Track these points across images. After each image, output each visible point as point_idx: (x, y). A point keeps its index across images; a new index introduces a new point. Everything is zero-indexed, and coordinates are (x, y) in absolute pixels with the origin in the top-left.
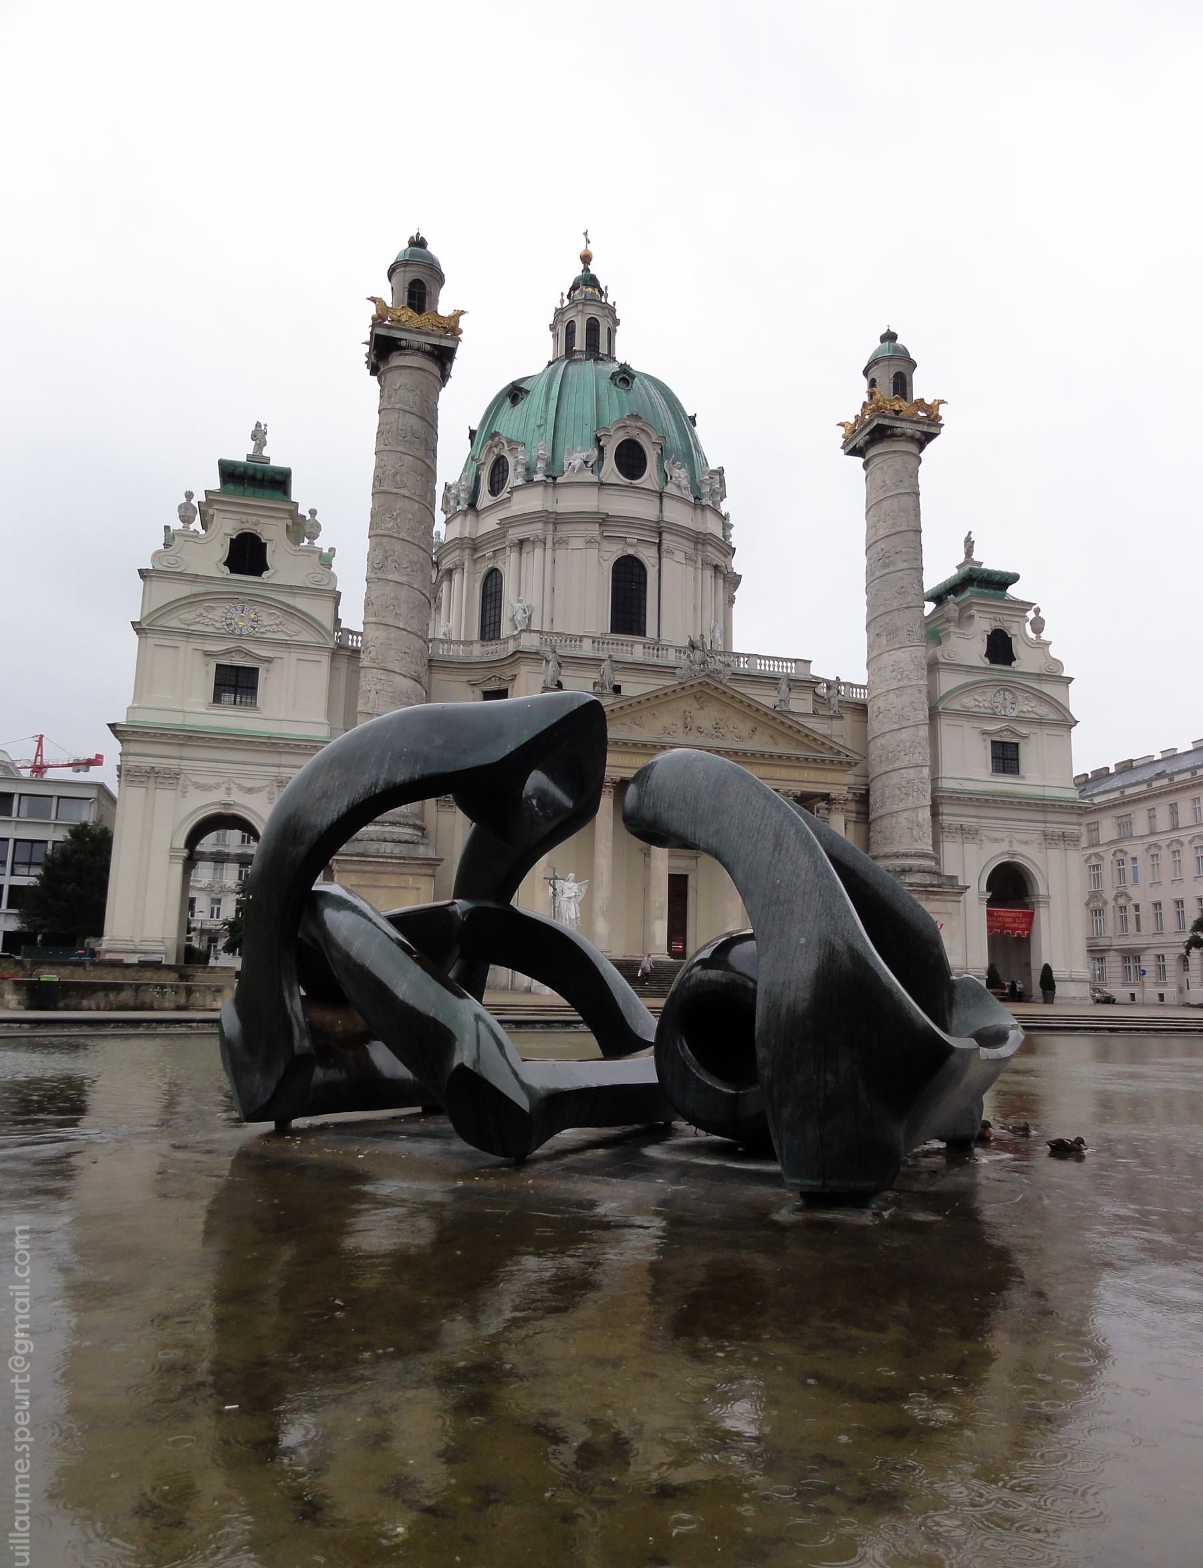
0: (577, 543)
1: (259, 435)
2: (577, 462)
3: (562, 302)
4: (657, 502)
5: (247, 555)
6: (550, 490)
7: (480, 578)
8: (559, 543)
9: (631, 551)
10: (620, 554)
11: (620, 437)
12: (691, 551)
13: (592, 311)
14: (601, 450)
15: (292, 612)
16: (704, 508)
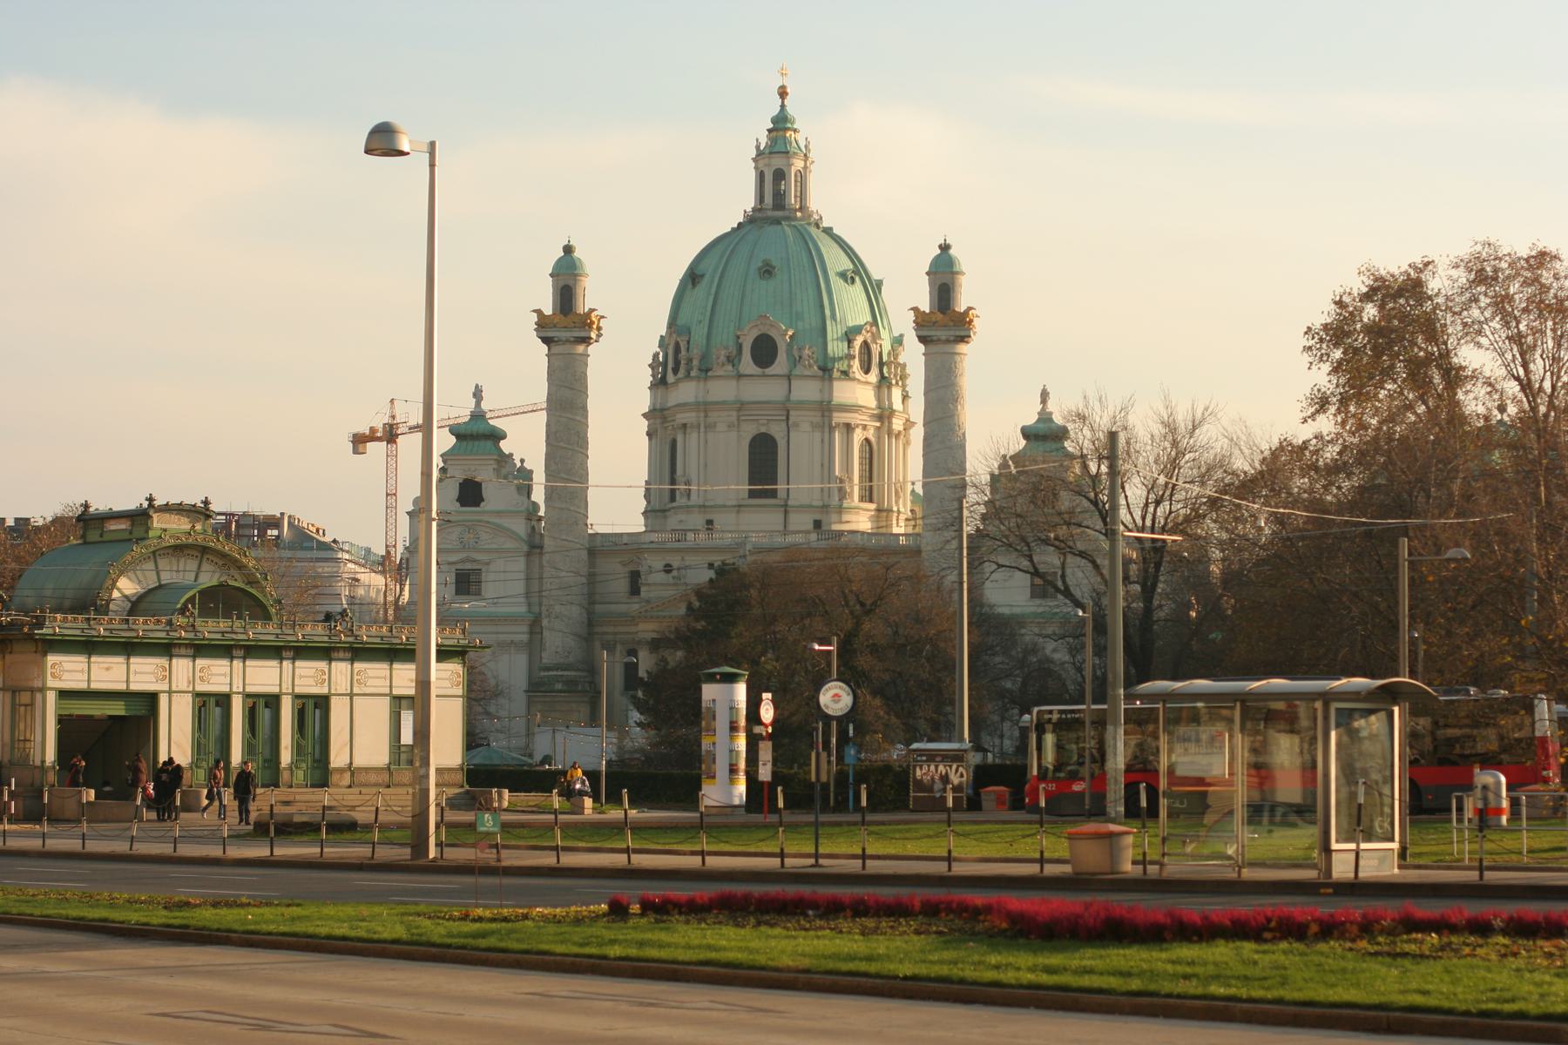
0: (721, 427)
1: (478, 394)
2: (722, 358)
3: (758, 147)
4: (786, 382)
5: (470, 493)
6: (702, 384)
7: (668, 440)
8: (710, 427)
9: (763, 430)
10: (755, 432)
11: (755, 333)
12: (818, 419)
13: (778, 162)
14: (740, 347)
15: (499, 529)
16: (831, 379)
